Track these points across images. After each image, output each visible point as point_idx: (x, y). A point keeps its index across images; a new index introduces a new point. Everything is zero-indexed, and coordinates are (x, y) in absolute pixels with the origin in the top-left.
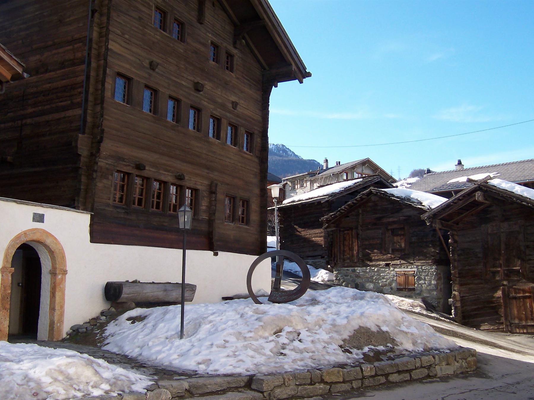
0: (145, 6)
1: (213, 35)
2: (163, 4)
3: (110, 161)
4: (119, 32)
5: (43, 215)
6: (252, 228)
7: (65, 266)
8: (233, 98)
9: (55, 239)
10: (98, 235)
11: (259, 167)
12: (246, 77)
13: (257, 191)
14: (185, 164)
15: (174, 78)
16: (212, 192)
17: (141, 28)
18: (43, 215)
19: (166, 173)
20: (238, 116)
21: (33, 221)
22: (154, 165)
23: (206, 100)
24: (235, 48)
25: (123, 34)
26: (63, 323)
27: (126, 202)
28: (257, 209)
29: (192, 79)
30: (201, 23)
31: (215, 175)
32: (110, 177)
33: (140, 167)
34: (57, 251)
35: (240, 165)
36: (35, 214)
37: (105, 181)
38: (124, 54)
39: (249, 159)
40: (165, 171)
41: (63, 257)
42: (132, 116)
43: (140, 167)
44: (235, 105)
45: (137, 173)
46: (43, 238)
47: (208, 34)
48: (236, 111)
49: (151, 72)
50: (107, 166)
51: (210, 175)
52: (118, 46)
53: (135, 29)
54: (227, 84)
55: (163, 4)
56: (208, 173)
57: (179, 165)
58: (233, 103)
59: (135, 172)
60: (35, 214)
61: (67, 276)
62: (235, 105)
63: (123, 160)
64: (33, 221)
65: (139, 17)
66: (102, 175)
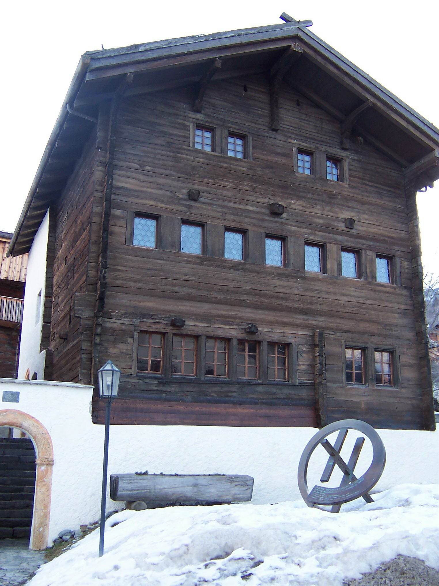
0: (178, 128)
1: (298, 140)
2: (208, 120)
3: (126, 321)
4: (135, 166)
5: (18, 394)
6: (404, 391)
7: (51, 454)
8: (346, 214)
9: (37, 421)
10: (103, 412)
11: (410, 302)
12: (370, 184)
13: (410, 335)
14: (260, 312)
15: (231, 205)
16: (316, 343)
17: (171, 154)
18: (18, 394)
19: (228, 327)
20: (358, 237)
21: (3, 401)
22: (199, 317)
23: (293, 223)
24: (344, 149)
25: (142, 166)
26: (48, 528)
27: (163, 370)
28: (413, 362)
29: (266, 200)
30: (275, 130)
31: (320, 321)
32: (129, 340)
33: (177, 323)
34: (39, 436)
35: (368, 302)
36: (5, 393)
37: (121, 346)
38: (145, 189)
39: (389, 293)
40: (225, 324)
41: (49, 443)
42: (162, 262)
43: (177, 323)
44: (350, 223)
45: (175, 331)
46: (19, 420)
47: (290, 140)
48: (354, 231)
49: (192, 203)
50: (123, 327)
51: (310, 322)
52: (133, 181)
53: (161, 157)
54: (333, 198)
55: (208, 120)
56: (307, 320)
57: (248, 313)
58: (345, 220)
59: (170, 330)
60: (5, 393)
61: (54, 467)
62: (350, 223)
63: (150, 316)
64: (3, 401)
65: (168, 142)
66: (115, 339)
